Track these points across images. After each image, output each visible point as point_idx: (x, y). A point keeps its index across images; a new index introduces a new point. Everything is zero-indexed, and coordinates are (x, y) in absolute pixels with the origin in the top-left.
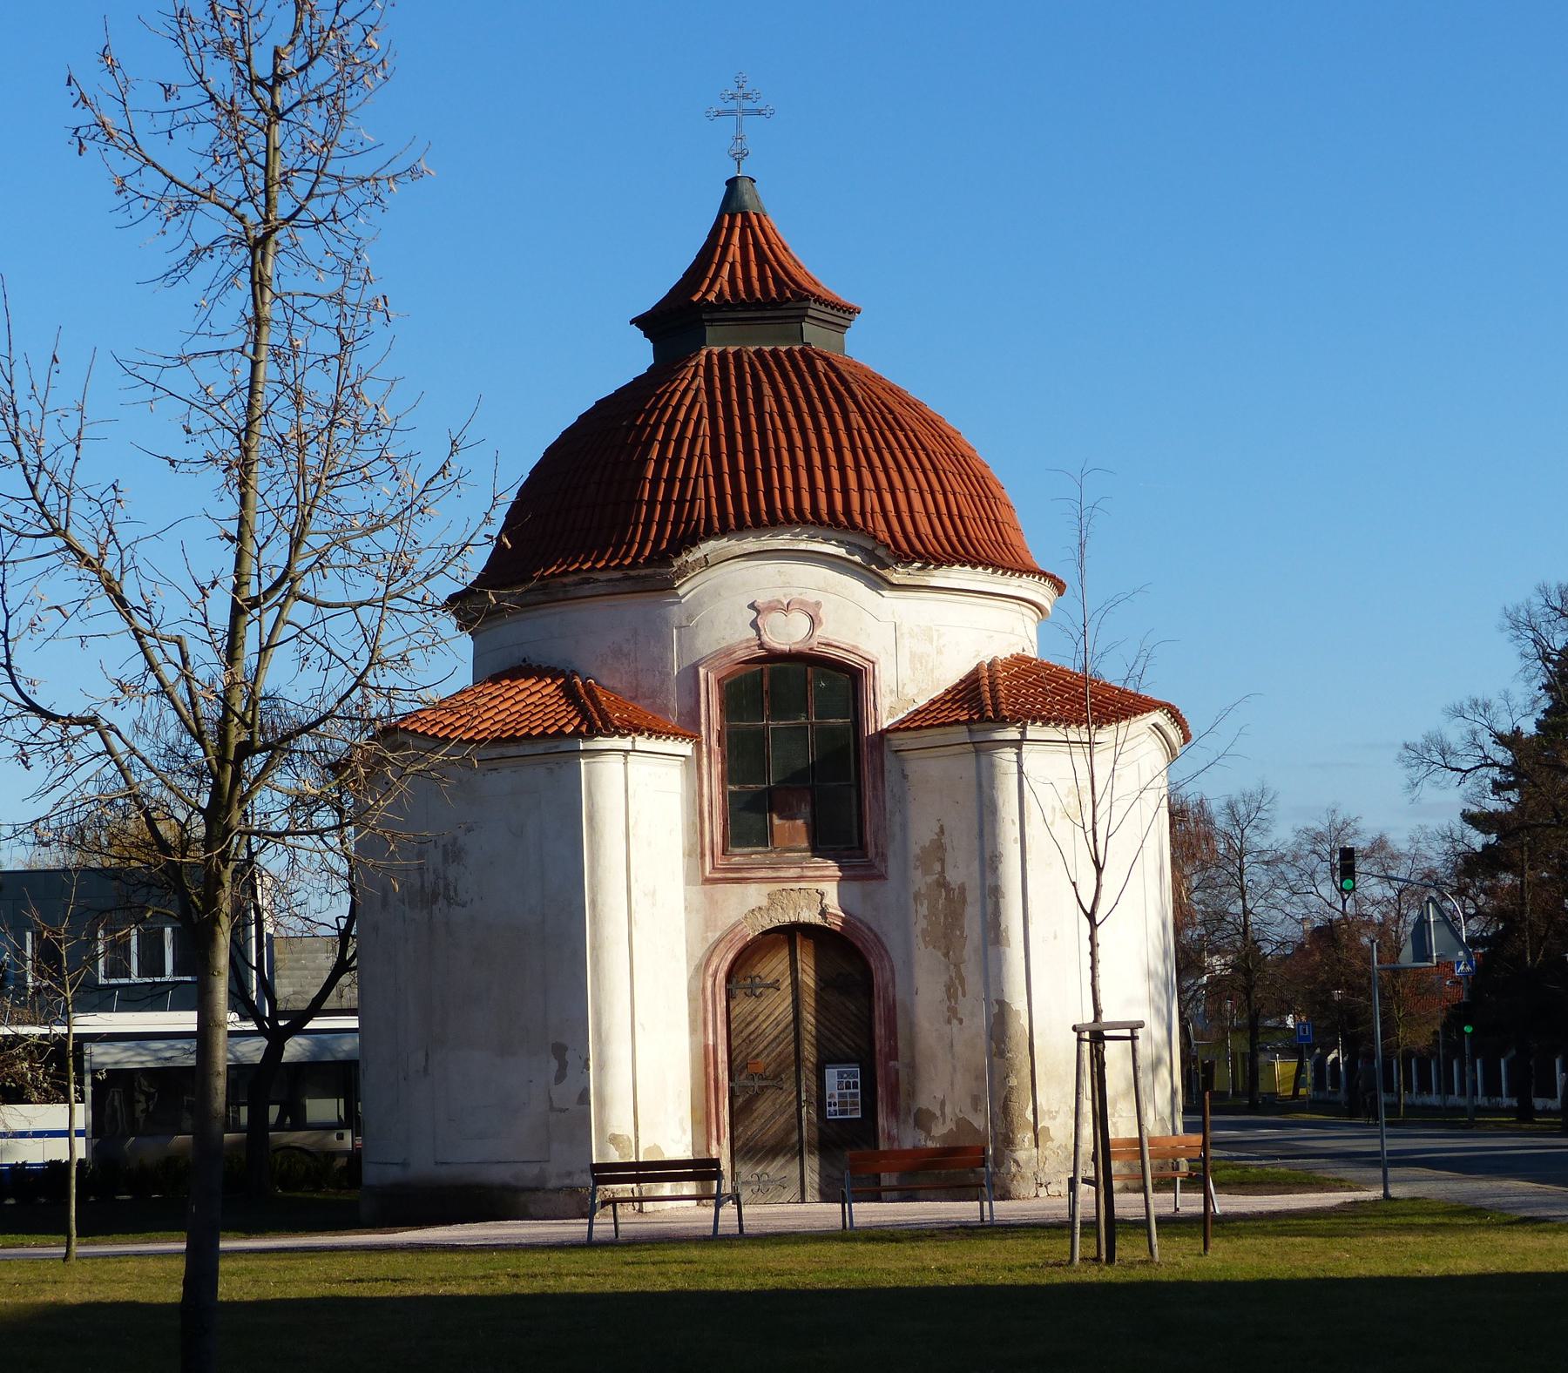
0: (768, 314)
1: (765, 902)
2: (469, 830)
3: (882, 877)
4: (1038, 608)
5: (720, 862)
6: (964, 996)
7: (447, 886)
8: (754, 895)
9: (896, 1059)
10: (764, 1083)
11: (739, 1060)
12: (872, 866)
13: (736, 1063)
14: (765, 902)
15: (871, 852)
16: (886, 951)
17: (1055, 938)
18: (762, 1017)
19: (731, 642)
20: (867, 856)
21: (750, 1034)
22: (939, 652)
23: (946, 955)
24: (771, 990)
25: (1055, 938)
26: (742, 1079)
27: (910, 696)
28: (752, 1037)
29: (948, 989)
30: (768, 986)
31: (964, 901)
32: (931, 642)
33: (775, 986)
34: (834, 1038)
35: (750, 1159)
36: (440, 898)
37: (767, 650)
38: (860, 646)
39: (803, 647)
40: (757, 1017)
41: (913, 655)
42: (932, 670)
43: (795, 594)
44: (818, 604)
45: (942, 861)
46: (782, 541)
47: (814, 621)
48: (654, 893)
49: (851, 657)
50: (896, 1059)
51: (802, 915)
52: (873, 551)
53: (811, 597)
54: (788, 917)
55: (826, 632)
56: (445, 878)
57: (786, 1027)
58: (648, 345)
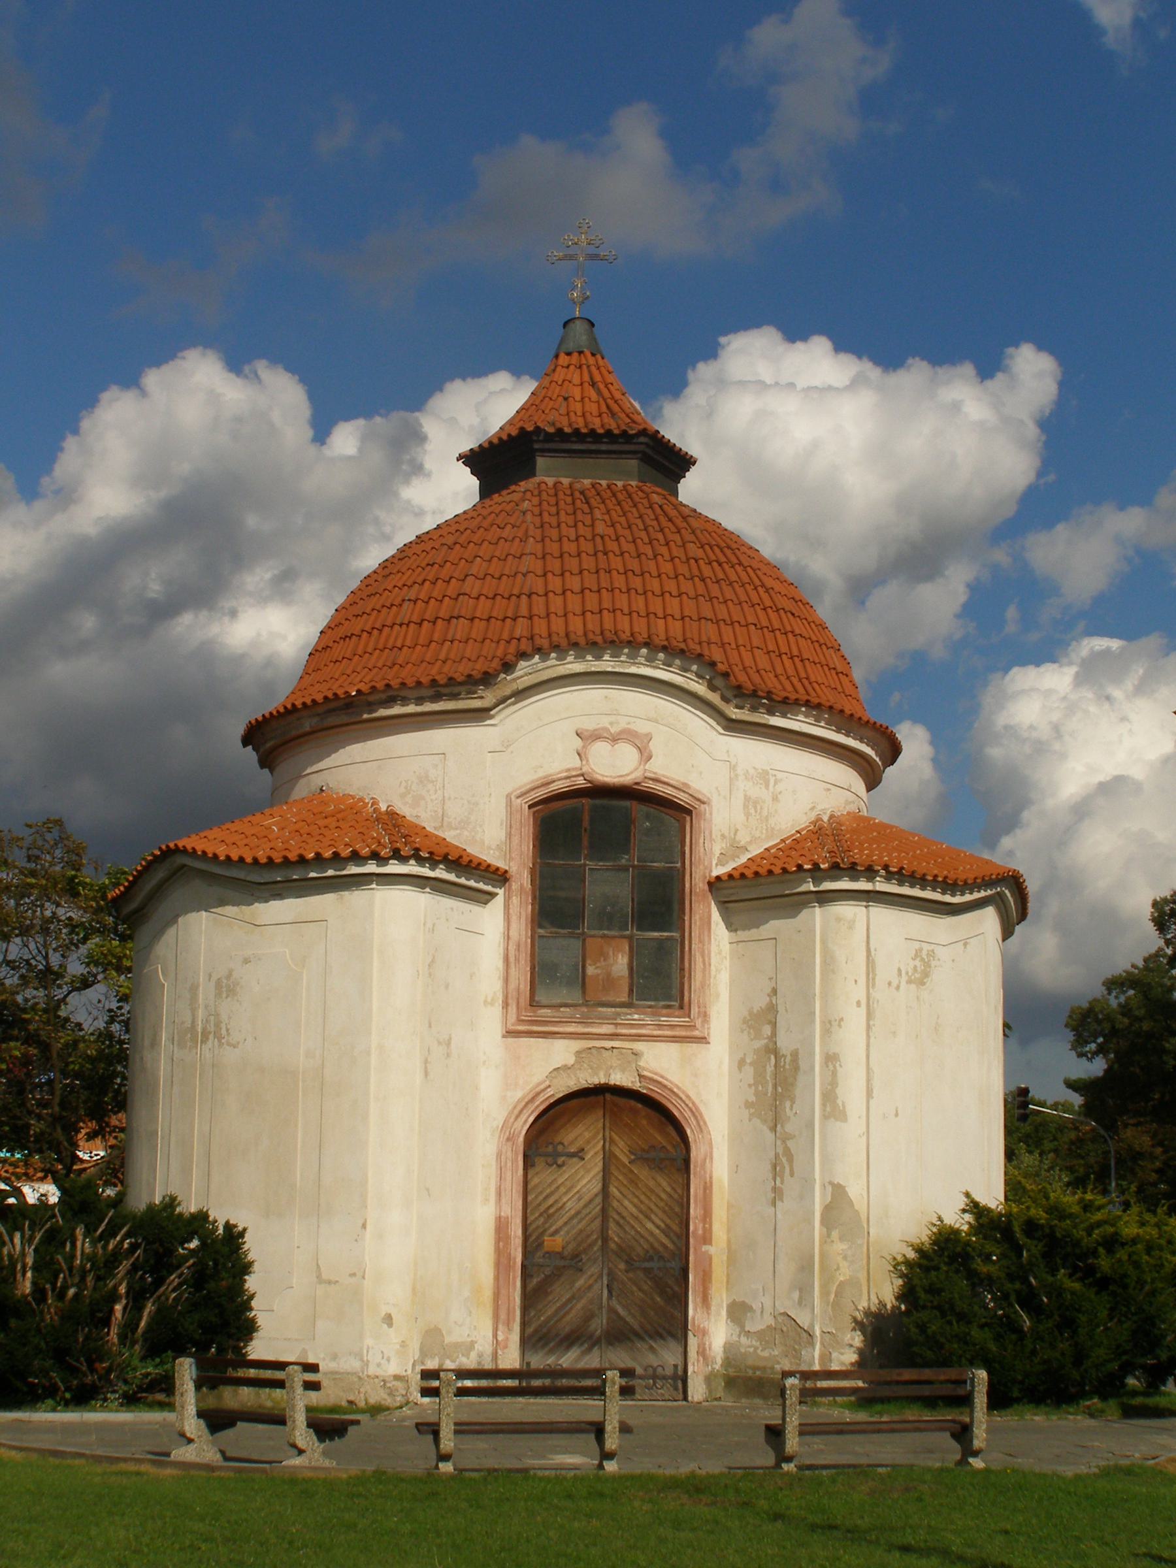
0: (604, 447)
1: (571, 1060)
2: (246, 961)
3: (703, 1040)
5: (527, 1015)
6: (792, 1175)
7: (218, 1025)
8: (562, 1052)
9: (710, 1244)
10: (562, 1263)
11: (534, 1237)
13: (531, 1240)
14: (571, 1060)
15: (694, 1011)
17: (897, 1115)
18: (563, 1190)
19: (551, 771)
21: (548, 1208)
22: (775, 799)
23: (774, 1129)
24: (575, 1160)
25: (897, 1115)
26: (538, 1258)
27: (743, 843)
28: (551, 1211)
29: (774, 1167)
30: (573, 1155)
31: (796, 1069)
32: (767, 786)
33: (579, 1154)
34: (641, 1216)
35: (543, 1347)
36: (211, 1037)
37: (590, 782)
38: (690, 784)
39: (628, 780)
40: (558, 1188)
41: (747, 799)
42: (767, 819)
43: (623, 723)
44: (649, 737)
45: (774, 1025)
46: (607, 664)
47: (645, 755)
48: (448, 1044)
49: (682, 795)
50: (710, 1244)
51: (612, 1077)
53: (642, 727)
54: (599, 1079)
56: (217, 1015)
57: (591, 1201)
58: (474, 482)
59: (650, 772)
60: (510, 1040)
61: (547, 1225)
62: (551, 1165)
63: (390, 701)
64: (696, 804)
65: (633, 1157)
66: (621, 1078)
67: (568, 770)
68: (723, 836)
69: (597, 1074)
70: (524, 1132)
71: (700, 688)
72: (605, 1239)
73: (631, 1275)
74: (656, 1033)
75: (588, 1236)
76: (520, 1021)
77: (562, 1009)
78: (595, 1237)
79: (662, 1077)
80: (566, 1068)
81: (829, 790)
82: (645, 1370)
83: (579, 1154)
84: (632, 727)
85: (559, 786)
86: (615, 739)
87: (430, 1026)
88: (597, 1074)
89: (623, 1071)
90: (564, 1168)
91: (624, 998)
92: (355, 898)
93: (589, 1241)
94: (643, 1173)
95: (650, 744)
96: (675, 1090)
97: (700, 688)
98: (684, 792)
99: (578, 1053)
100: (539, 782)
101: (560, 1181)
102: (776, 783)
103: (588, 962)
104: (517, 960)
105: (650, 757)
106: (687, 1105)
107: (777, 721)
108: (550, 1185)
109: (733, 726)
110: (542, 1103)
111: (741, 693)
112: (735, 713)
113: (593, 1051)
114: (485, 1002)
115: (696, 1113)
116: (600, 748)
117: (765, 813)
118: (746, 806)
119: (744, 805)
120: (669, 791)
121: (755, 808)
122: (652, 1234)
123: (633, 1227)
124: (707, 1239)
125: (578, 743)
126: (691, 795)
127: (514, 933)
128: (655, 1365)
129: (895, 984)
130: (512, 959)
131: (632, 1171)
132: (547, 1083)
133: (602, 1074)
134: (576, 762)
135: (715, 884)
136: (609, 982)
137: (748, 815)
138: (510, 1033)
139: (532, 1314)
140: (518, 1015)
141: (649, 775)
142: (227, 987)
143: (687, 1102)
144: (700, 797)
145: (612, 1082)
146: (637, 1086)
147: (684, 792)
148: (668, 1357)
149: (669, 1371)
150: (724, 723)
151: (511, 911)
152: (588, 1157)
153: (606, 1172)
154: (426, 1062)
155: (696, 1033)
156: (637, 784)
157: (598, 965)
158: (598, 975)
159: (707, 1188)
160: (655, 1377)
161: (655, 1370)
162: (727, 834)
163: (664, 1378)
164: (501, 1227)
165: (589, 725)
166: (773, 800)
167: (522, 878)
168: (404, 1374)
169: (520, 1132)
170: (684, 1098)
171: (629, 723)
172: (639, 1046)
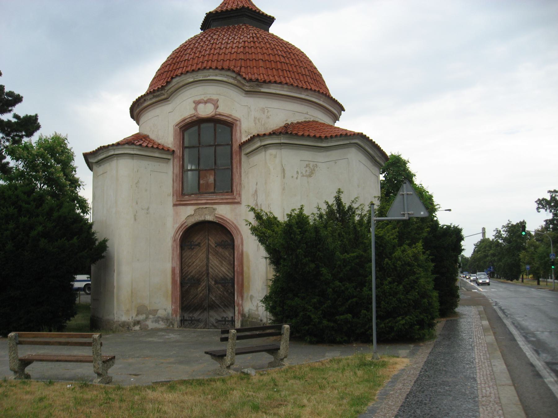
1: (193, 213)
3: (239, 203)
4: (334, 115)
8: (190, 210)
11: (184, 274)
12: (235, 199)
13: (183, 274)
14: (193, 213)
16: (240, 232)
19: (185, 116)
20: (234, 195)
24: (197, 246)
28: (190, 264)
32: (264, 113)
33: (199, 245)
38: (233, 115)
41: (255, 118)
43: (208, 97)
46: (200, 76)
49: (229, 119)
51: (206, 217)
52: (236, 78)
53: (215, 97)
54: (202, 218)
55: (221, 110)
59: (217, 112)
60: (175, 207)
61: (189, 270)
62: (190, 249)
64: (235, 122)
65: (216, 245)
66: (209, 218)
67: (191, 115)
68: (246, 132)
69: (201, 217)
70: (179, 238)
72: (208, 274)
73: (216, 286)
74: (220, 201)
75: (202, 273)
76: (177, 201)
77: (192, 196)
78: (204, 273)
79: (223, 216)
80: (191, 216)
81: (295, 114)
82: (222, 318)
83: (199, 245)
84: (212, 97)
86: (206, 102)
87: (137, 203)
88: (201, 217)
89: (210, 215)
90: (194, 250)
91: (212, 190)
93: (203, 275)
94: (220, 250)
95: (218, 103)
96: (228, 221)
98: (230, 117)
99: (195, 211)
100: (182, 120)
101: (193, 254)
102: (268, 112)
103: (201, 179)
104: (176, 180)
105: (218, 107)
106: (232, 226)
107: (263, 90)
108: (190, 255)
109: (248, 93)
110: (184, 228)
112: (247, 88)
113: (200, 209)
114: (168, 195)
115: (236, 228)
116: (201, 106)
117: (263, 122)
118: (254, 121)
119: (254, 120)
120: (224, 118)
121: (259, 121)
122: (223, 271)
123: (217, 269)
125: (194, 105)
126: (232, 118)
127: (175, 171)
128: (225, 316)
129: (295, 176)
130: (175, 180)
131: (216, 250)
132: (185, 221)
133: (203, 217)
134: (192, 112)
137: (256, 124)
138: (175, 205)
139: (184, 299)
140: (177, 198)
141: (217, 113)
143: (232, 225)
144: (236, 119)
145: (206, 219)
146: (215, 220)
147: (230, 117)
148: (229, 315)
149: (230, 319)
150: (244, 92)
151: (174, 164)
152: (201, 245)
154: (135, 216)
155: (236, 201)
156: (213, 116)
157: (204, 180)
158: (204, 183)
160: (225, 321)
161: (225, 318)
162: (247, 131)
163: (228, 321)
164: (173, 270)
165: (197, 99)
166: (267, 118)
168: (128, 321)
169: (178, 238)
170: (231, 223)
171: (210, 96)
172: (215, 206)
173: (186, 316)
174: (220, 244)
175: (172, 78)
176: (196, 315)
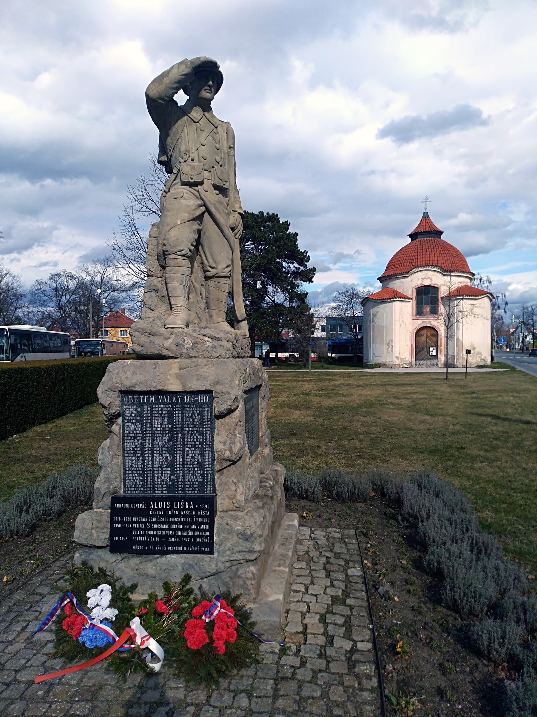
8: (420, 322)
26: (417, 349)
33: (423, 335)
43: (428, 276)
47: (431, 281)
53: (431, 277)
55: (433, 282)
63: (397, 275)
66: (428, 325)
71: (439, 270)
85: (420, 286)
92: (390, 304)
94: (432, 337)
97: (439, 270)
111: (445, 271)
124: (441, 346)
135: (442, 298)
136: (427, 312)
142: (375, 316)
153: (427, 338)
159: (441, 339)
164: (412, 345)
165: (423, 277)
167: (414, 299)
173: (417, 362)
174: (432, 335)
175: (413, 268)
176: (422, 362)
